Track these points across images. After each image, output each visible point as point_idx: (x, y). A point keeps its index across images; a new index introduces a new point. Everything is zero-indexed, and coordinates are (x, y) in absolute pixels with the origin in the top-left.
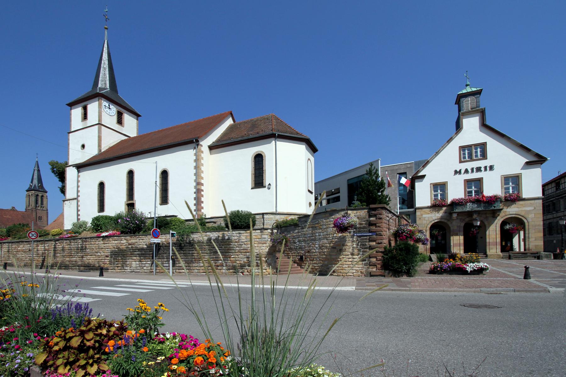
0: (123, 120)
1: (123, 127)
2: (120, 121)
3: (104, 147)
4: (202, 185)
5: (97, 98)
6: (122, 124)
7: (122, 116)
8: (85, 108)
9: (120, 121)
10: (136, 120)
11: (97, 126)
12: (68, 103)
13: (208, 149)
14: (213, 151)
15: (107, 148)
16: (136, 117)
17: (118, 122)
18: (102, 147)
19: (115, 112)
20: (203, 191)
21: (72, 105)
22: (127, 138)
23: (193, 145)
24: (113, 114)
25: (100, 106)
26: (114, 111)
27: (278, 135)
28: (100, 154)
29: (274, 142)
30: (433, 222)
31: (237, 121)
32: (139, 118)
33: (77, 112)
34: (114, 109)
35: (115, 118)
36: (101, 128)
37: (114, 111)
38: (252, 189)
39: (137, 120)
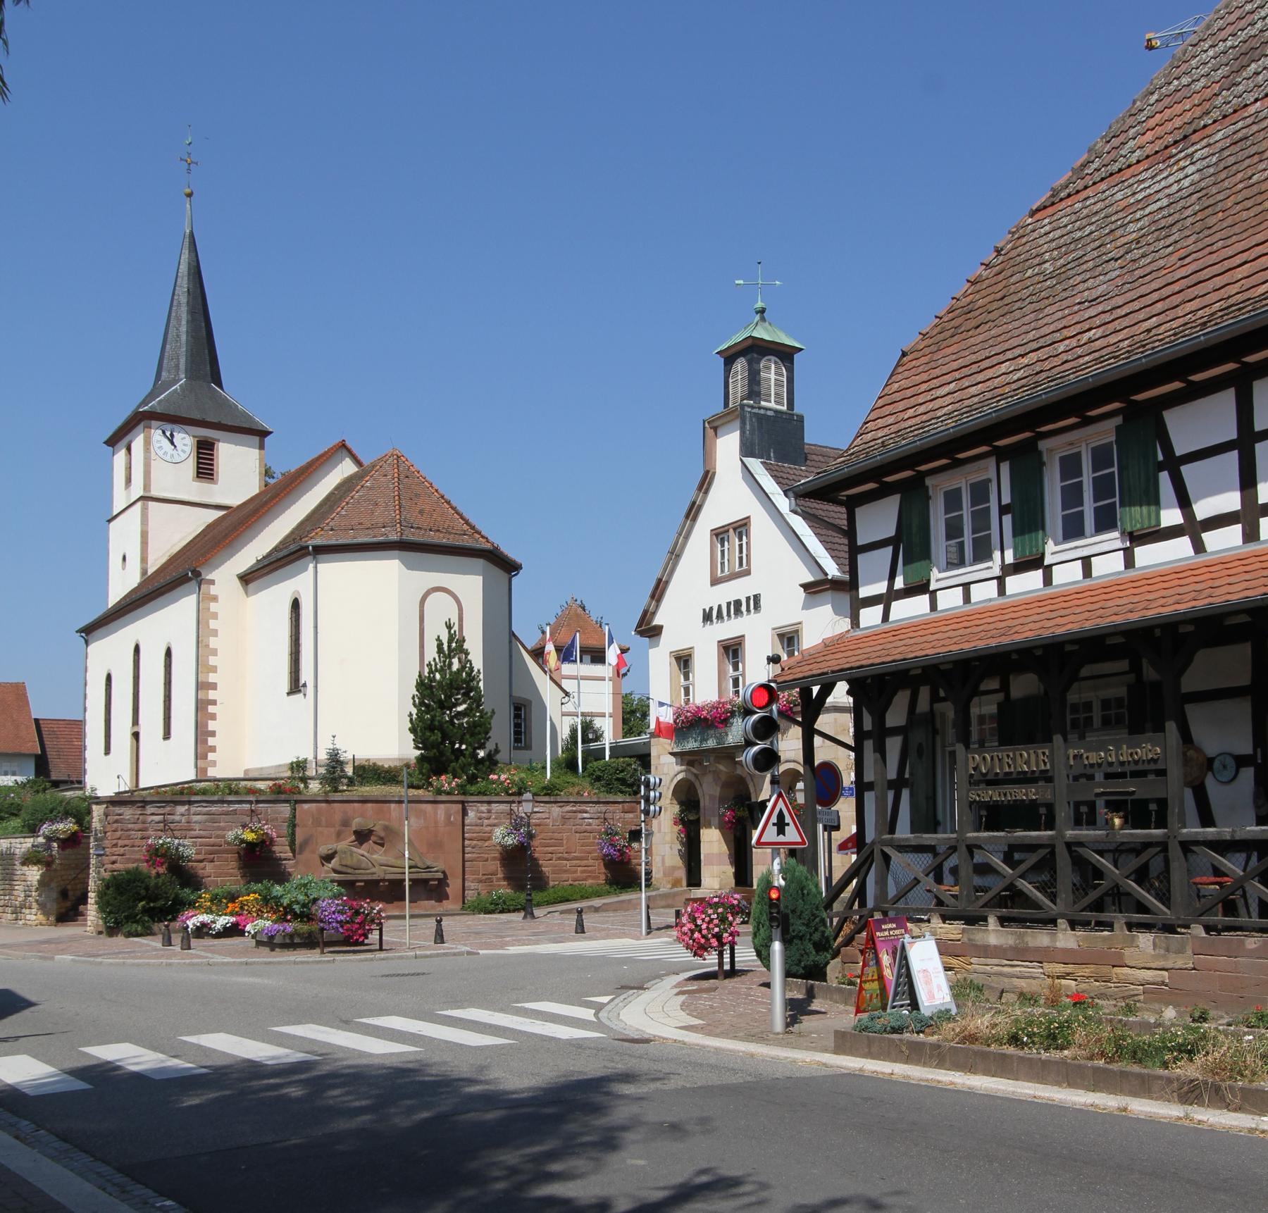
0: (215, 463)
1: (216, 483)
2: (205, 470)
3: (156, 560)
4: (213, 686)
5: (141, 426)
6: (212, 475)
7: (212, 450)
8: (129, 449)
9: (205, 470)
10: (257, 451)
11: (139, 504)
12: (105, 439)
13: (237, 582)
14: (251, 586)
15: (164, 560)
16: (257, 439)
17: (198, 473)
18: (150, 563)
19: (188, 449)
20: (214, 703)
21: (113, 441)
22: (221, 513)
23: (193, 584)
24: (184, 456)
25: (147, 443)
26: (184, 445)
27: (313, 547)
28: (147, 580)
29: (311, 566)
30: (675, 781)
31: (366, 462)
32: (267, 440)
33: (120, 458)
34: (185, 441)
35: (190, 466)
36: (147, 509)
37: (184, 445)
38: (289, 694)
39: (262, 447)
